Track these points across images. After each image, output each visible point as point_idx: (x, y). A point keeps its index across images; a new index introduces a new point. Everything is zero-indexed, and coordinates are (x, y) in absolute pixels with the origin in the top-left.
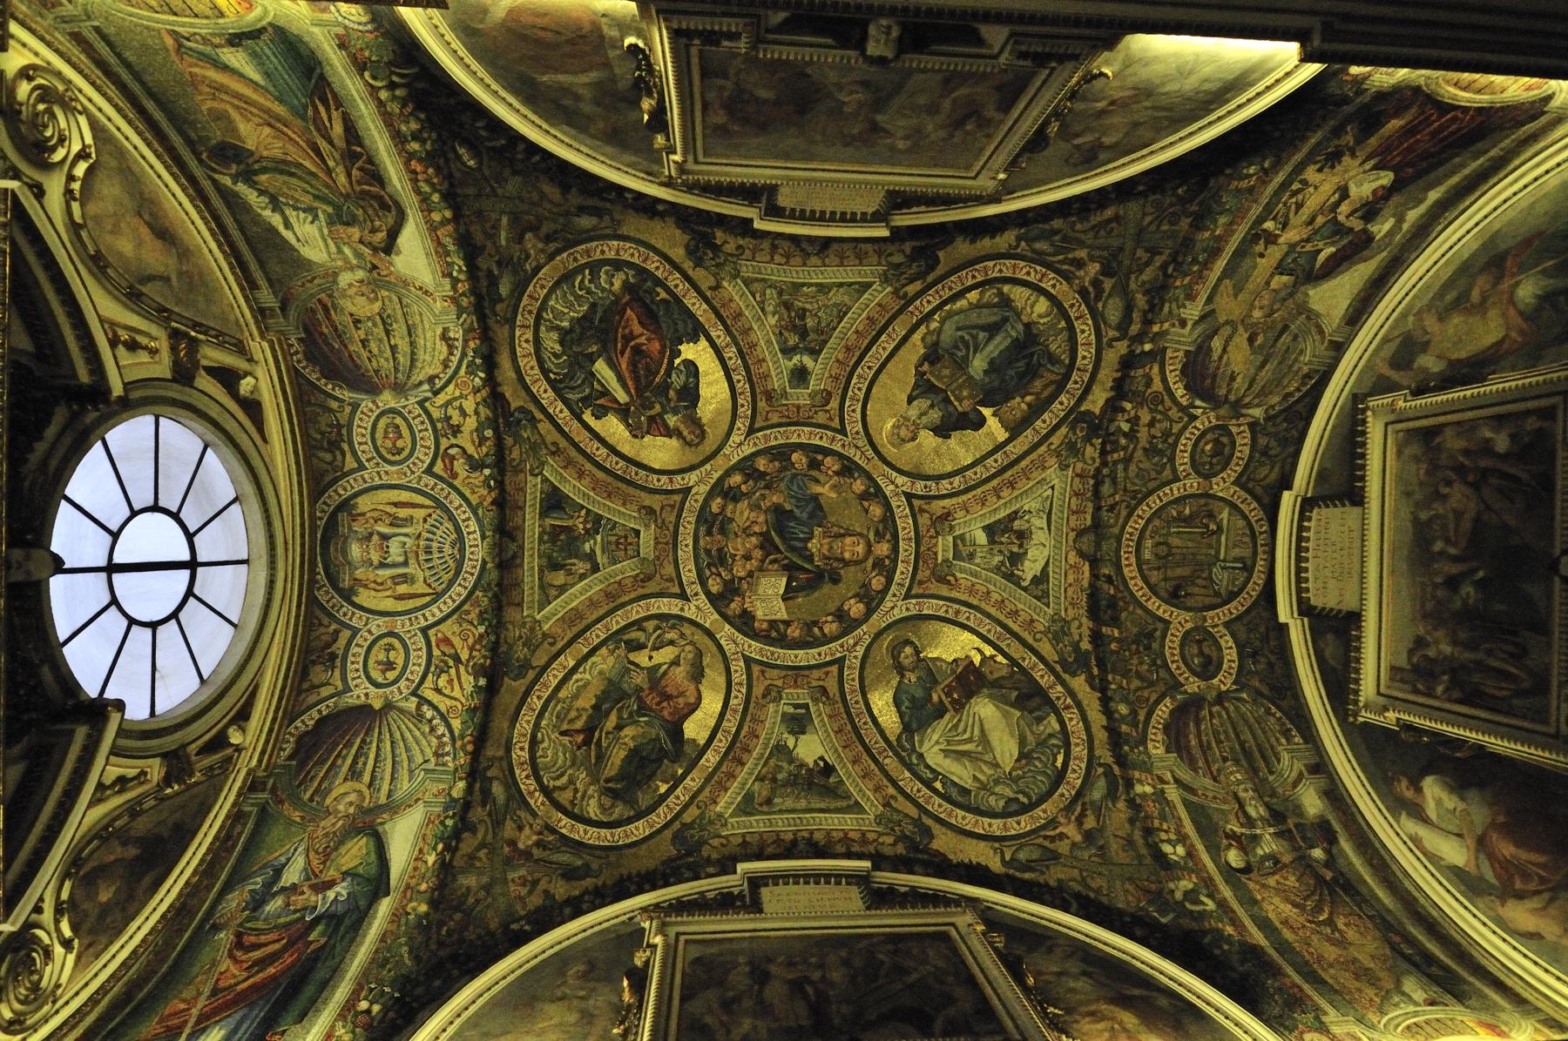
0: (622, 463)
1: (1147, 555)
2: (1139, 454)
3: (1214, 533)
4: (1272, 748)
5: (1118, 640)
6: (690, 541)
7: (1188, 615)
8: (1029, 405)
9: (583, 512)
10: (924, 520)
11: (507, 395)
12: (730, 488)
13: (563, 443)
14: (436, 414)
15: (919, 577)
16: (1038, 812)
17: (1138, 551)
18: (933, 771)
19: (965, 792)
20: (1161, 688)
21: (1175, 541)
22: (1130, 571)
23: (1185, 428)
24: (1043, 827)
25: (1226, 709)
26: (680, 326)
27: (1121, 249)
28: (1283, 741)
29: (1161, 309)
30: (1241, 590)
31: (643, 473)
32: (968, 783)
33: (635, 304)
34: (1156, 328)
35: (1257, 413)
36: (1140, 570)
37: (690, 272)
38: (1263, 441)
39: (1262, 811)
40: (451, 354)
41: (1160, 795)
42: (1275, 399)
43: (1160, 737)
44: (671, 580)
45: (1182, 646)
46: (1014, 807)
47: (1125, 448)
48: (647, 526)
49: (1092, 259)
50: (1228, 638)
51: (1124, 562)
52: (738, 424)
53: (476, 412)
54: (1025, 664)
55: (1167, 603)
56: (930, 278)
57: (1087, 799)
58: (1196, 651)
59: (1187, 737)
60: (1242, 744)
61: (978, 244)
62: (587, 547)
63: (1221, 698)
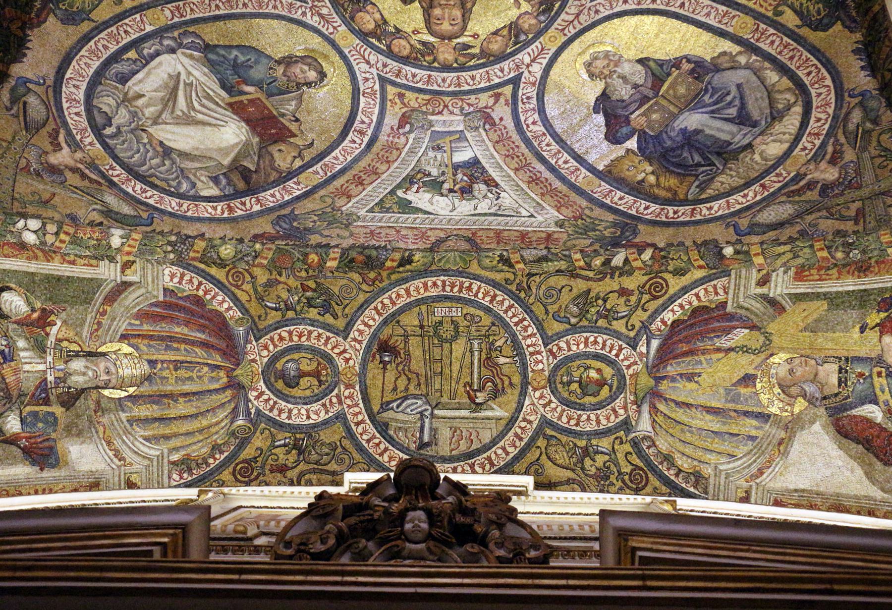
1: (441, 311)
2: (580, 285)
3: (472, 399)
4: (167, 438)
5: (322, 262)
7: (356, 363)
8: (643, 181)
10: (485, 99)
15: (409, 95)
16: (90, 138)
17: (447, 298)
18: (153, 57)
19: (124, 79)
20: (254, 308)
21: (459, 348)
22: (417, 288)
23: (617, 335)
24: (69, 133)
25: (224, 389)
28: (175, 457)
30: (391, 440)
32: (134, 86)
35: (644, 425)
36: (419, 302)
38: (605, 444)
39: (78, 381)
41: (105, 254)
42: (663, 444)
43: (187, 289)
45: (313, 350)
46: (100, 120)
47: (588, 266)
50: (323, 416)
51: (430, 281)
54: (290, 183)
55: (374, 336)
56: (805, 32)
57: (104, 188)
58: (305, 367)
59: (187, 324)
60: (171, 396)
61: (852, 58)
63: (237, 387)
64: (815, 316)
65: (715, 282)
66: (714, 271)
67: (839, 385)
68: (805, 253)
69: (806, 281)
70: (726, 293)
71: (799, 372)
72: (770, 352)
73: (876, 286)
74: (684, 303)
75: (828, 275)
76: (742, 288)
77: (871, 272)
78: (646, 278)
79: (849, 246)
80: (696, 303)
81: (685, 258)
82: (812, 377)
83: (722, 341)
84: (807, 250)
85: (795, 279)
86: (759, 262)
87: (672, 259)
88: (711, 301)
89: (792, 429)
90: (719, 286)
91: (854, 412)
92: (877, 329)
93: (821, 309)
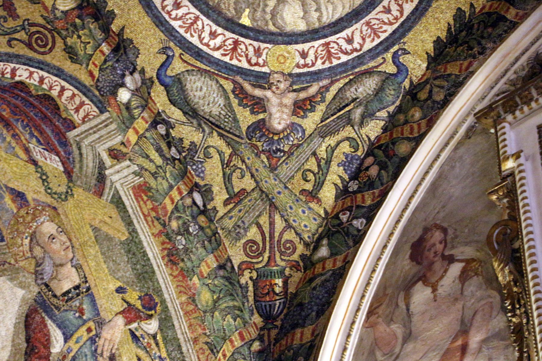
27: (273, 169)
29: (159, 150)
34: (141, 125)
49: (293, 127)
61: (448, 17)
64: (111, 232)
65: (87, 101)
66: (97, 93)
67: (64, 294)
68: (161, 184)
69: (138, 202)
70: (84, 122)
71: (56, 246)
72: (55, 204)
73: (161, 281)
74: (46, 81)
75: (153, 222)
76: (97, 136)
77: (172, 268)
78: (41, 21)
79: (184, 231)
80: (54, 93)
81: (89, 51)
82: (58, 262)
83: (37, 149)
84: (165, 185)
85: (134, 188)
86: (131, 139)
87: (79, 37)
88: (66, 109)
89: (5, 270)
90: (86, 107)
91: (49, 322)
92: (125, 305)
93: (120, 235)
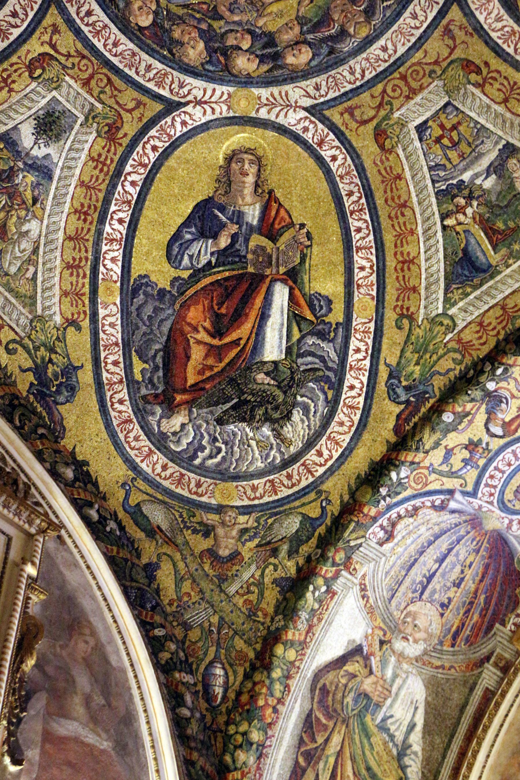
0: (354, 223)
6: (375, 50)
9: (449, 222)
11: (391, 424)
12: (262, 59)
13: (390, 317)
14: (472, 475)
26: (148, 310)
31: (343, 188)
33: (178, 385)
37: (89, 367)
40: (400, 517)
44: (447, 31)
48: (402, 124)
52: (179, 130)
53: (437, 444)
62: (489, 183)
